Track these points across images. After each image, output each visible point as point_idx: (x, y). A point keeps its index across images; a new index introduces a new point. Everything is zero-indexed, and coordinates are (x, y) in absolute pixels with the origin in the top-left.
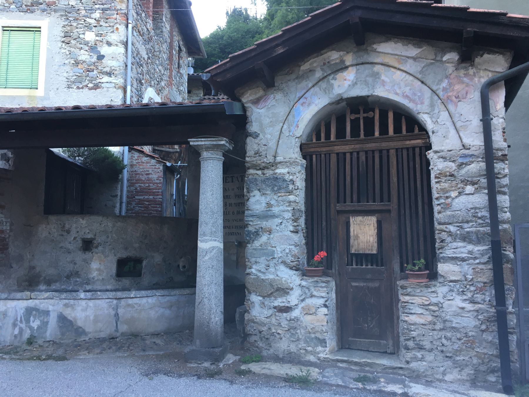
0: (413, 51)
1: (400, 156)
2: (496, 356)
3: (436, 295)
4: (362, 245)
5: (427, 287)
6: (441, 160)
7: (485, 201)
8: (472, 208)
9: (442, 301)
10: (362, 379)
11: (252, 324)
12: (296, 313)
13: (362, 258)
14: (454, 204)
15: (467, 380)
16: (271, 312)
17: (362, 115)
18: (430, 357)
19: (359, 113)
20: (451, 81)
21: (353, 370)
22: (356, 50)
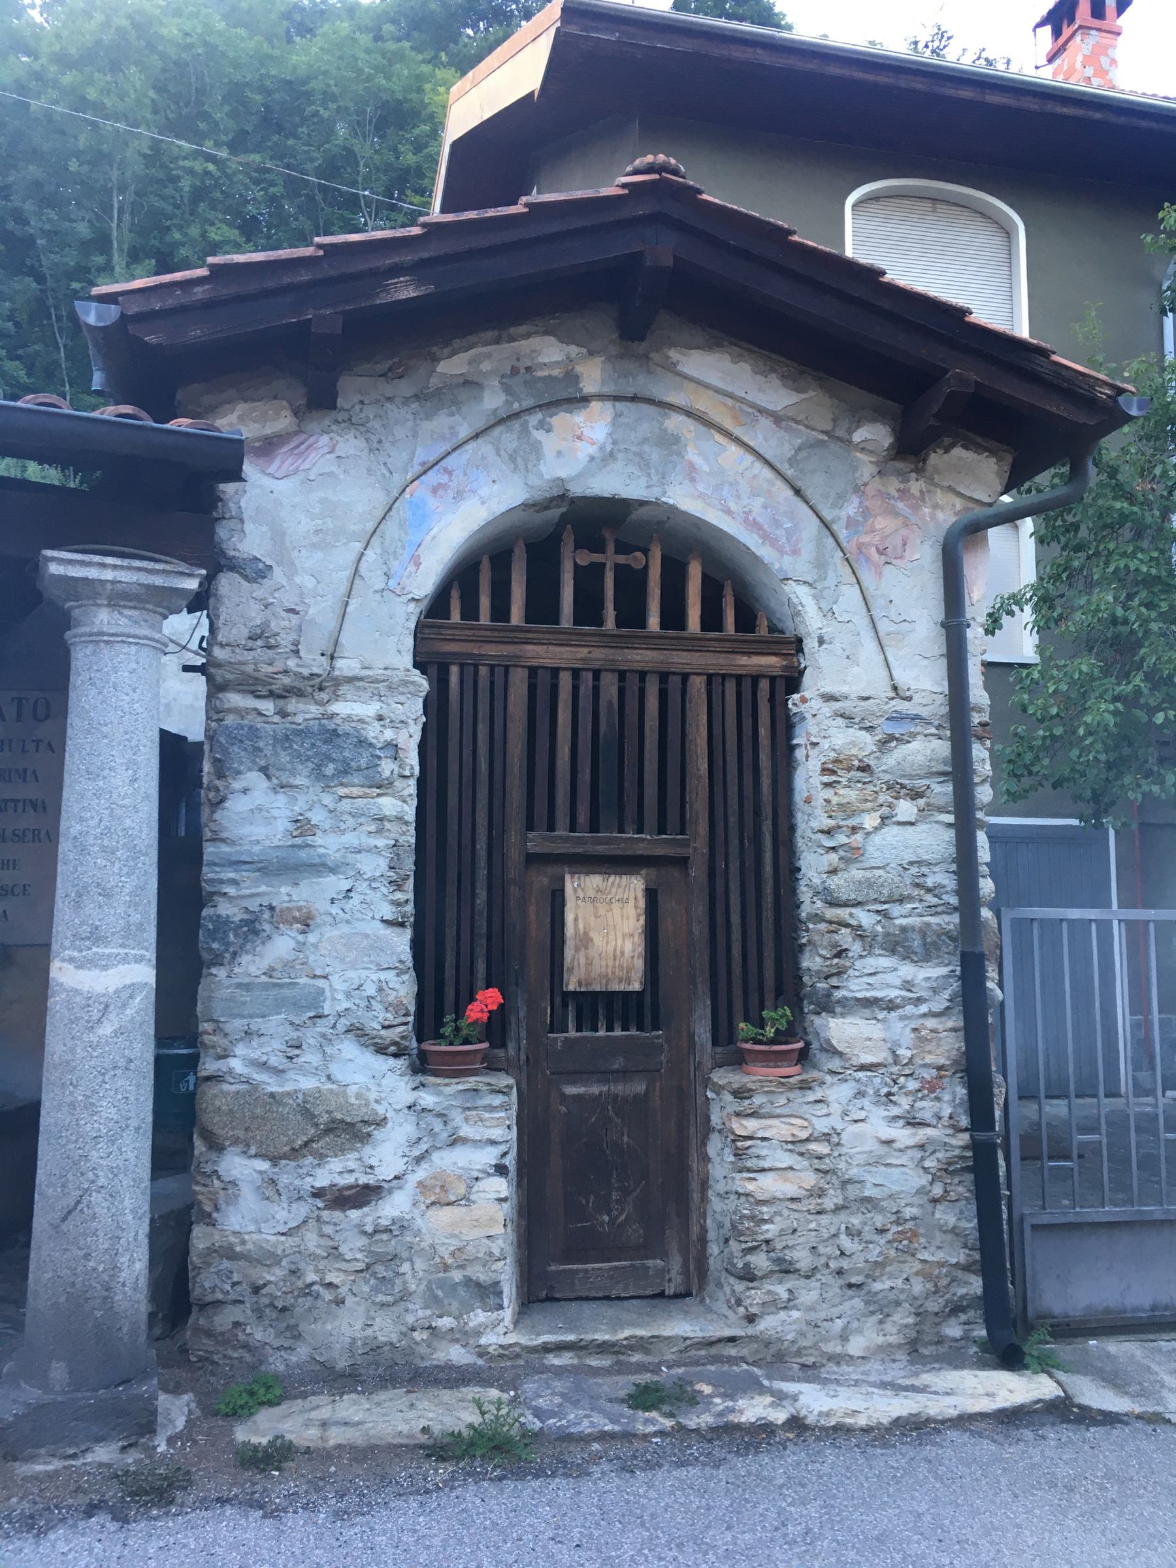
0: (777, 396)
1: (716, 699)
2: (967, 1268)
3: (825, 1111)
4: (598, 968)
5: (805, 1086)
6: (840, 721)
7: (944, 845)
8: (911, 863)
9: (839, 1127)
10: (645, 1398)
11: (226, 1264)
12: (393, 1207)
13: (598, 1006)
14: (870, 849)
15: (899, 1346)
16: (302, 1210)
17: (610, 559)
18: (809, 1294)
19: (602, 550)
20: (867, 503)
21: (596, 1372)
22: (613, 350)
